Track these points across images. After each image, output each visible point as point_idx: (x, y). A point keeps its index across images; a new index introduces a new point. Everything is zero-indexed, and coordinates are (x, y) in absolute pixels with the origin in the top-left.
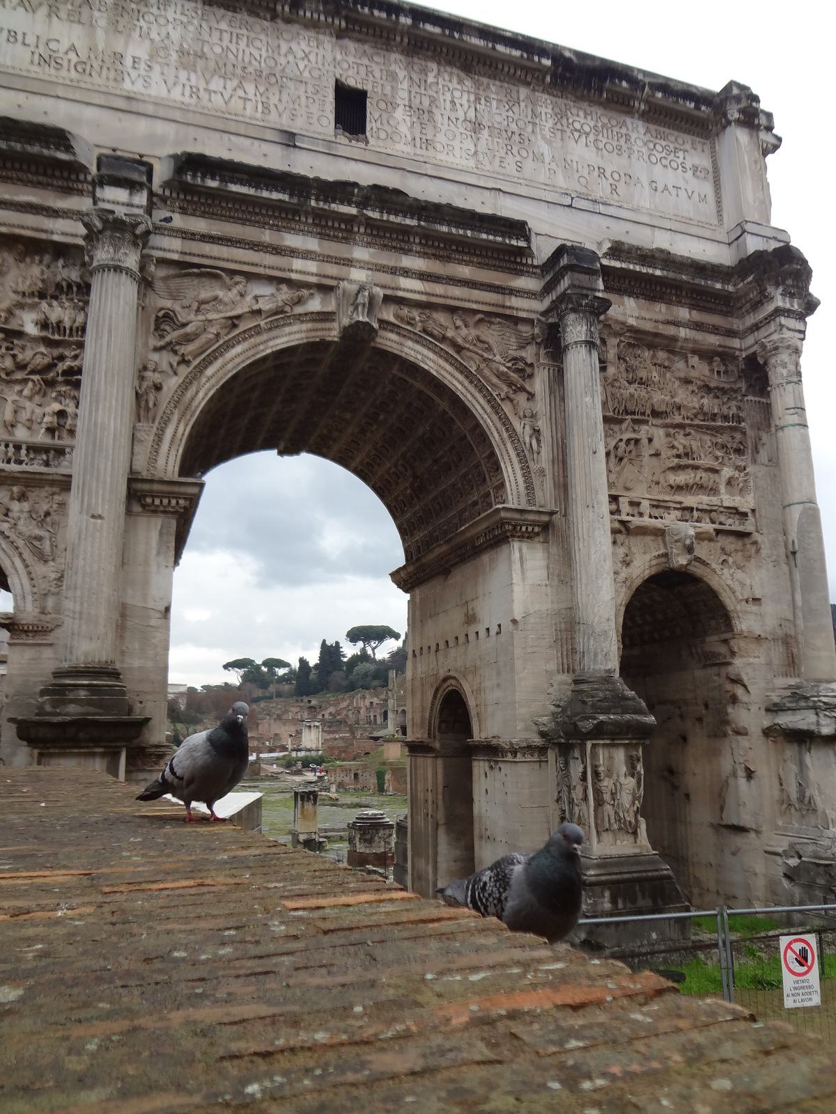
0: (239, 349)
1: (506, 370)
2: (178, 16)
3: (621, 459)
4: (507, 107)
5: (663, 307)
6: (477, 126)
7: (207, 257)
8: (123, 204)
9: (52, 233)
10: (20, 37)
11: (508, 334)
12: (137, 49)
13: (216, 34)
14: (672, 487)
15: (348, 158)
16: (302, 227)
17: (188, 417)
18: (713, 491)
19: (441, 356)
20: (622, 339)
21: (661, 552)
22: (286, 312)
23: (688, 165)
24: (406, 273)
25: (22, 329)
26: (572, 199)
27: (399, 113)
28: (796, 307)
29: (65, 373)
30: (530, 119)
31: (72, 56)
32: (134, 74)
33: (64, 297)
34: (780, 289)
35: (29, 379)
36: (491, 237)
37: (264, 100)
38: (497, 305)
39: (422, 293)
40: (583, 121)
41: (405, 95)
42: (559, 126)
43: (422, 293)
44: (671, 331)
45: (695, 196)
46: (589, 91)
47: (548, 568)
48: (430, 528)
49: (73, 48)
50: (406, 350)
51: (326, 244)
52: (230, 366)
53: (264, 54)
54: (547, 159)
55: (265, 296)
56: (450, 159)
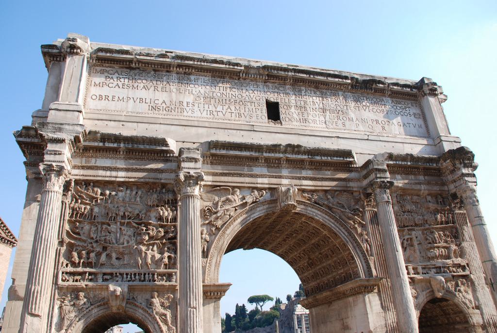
1: (351, 215)
2: (202, 83)
3: (406, 248)
4: (335, 101)
6: (324, 110)
7: (223, 182)
8: (192, 168)
9: (161, 179)
10: (144, 100)
11: (350, 199)
12: (190, 99)
14: (429, 258)
15: (275, 133)
16: (260, 164)
17: (221, 253)
18: (448, 257)
19: (323, 213)
20: (397, 193)
21: (430, 290)
22: (257, 202)
23: (411, 113)
26: (368, 136)
27: (293, 110)
29: (169, 239)
30: (345, 104)
31: (164, 105)
32: (188, 109)
34: (462, 165)
36: (338, 158)
37: (239, 112)
38: (344, 187)
39: (312, 186)
40: (366, 102)
41: (294, 102)
42: (357, 105)
43: (312, 186)
45: (417, 126)
46: (367, 89)
47: (382, 304)
48: (318, 281)
49: (164, 102)
50: (308, 211)
51: (270, 169)
52: (236, 228)
53: (236, 93)
54: (354, 120)
56: (316, 125)
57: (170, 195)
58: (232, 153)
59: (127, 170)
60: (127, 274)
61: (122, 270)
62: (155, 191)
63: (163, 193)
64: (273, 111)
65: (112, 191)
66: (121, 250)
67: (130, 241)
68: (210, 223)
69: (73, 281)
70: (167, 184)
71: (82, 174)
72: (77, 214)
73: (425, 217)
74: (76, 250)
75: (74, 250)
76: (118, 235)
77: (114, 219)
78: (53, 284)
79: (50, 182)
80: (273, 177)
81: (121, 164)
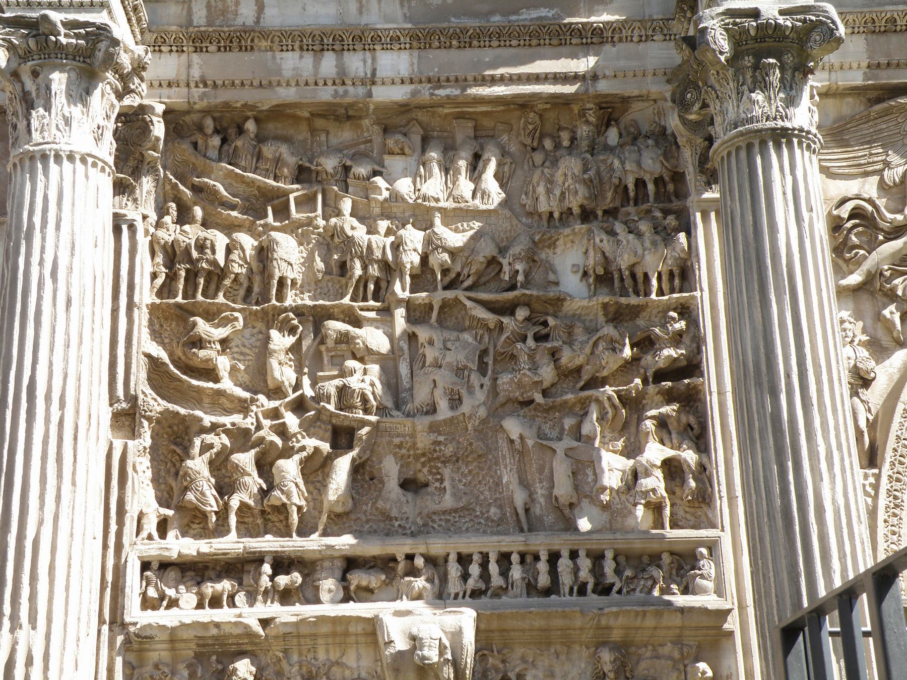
25: (552, 293)
29: (660, 376)
33: (631, 209)
35: (591, 397)
57: (645, 154)
60: (464, 560)
62: (566, 143)
63: (607, 148)
65: (353, 157)
66: (424, 441)
67: (464, 392)
69: (200, 606)
70: (626, 101)
71: (196, 73)
72: (192, 276)
74: (205, 448)
75: (196, 450)
76: (404, 369)
77: (377, 288)
78: (101, 622)
79: (48, 108)
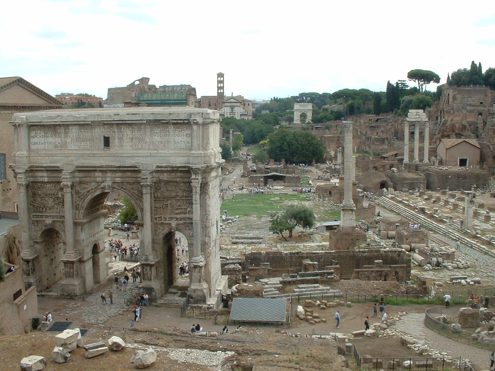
0: (90, 196)
5: (173, 174)
12: (69, 140)
13: (81, 132)
18: (185, 213)
23: (185, 134)
24: (117, 177)
27: (116, 139)
28: (197, 177)
31: (59, 145)
32: (69, 145)
41: (117, 135)
44: (175, 180)
45: (186, 142)
51: (103, 174)
55: (93, 185)
56: (127, 148)
58: (84, 169)
59: (47, 177)
61: (50, 215)
64: (107, 142)
68: (79, 197)
73: (178, 194)
80: (103, 177)
81: (45, 174)
